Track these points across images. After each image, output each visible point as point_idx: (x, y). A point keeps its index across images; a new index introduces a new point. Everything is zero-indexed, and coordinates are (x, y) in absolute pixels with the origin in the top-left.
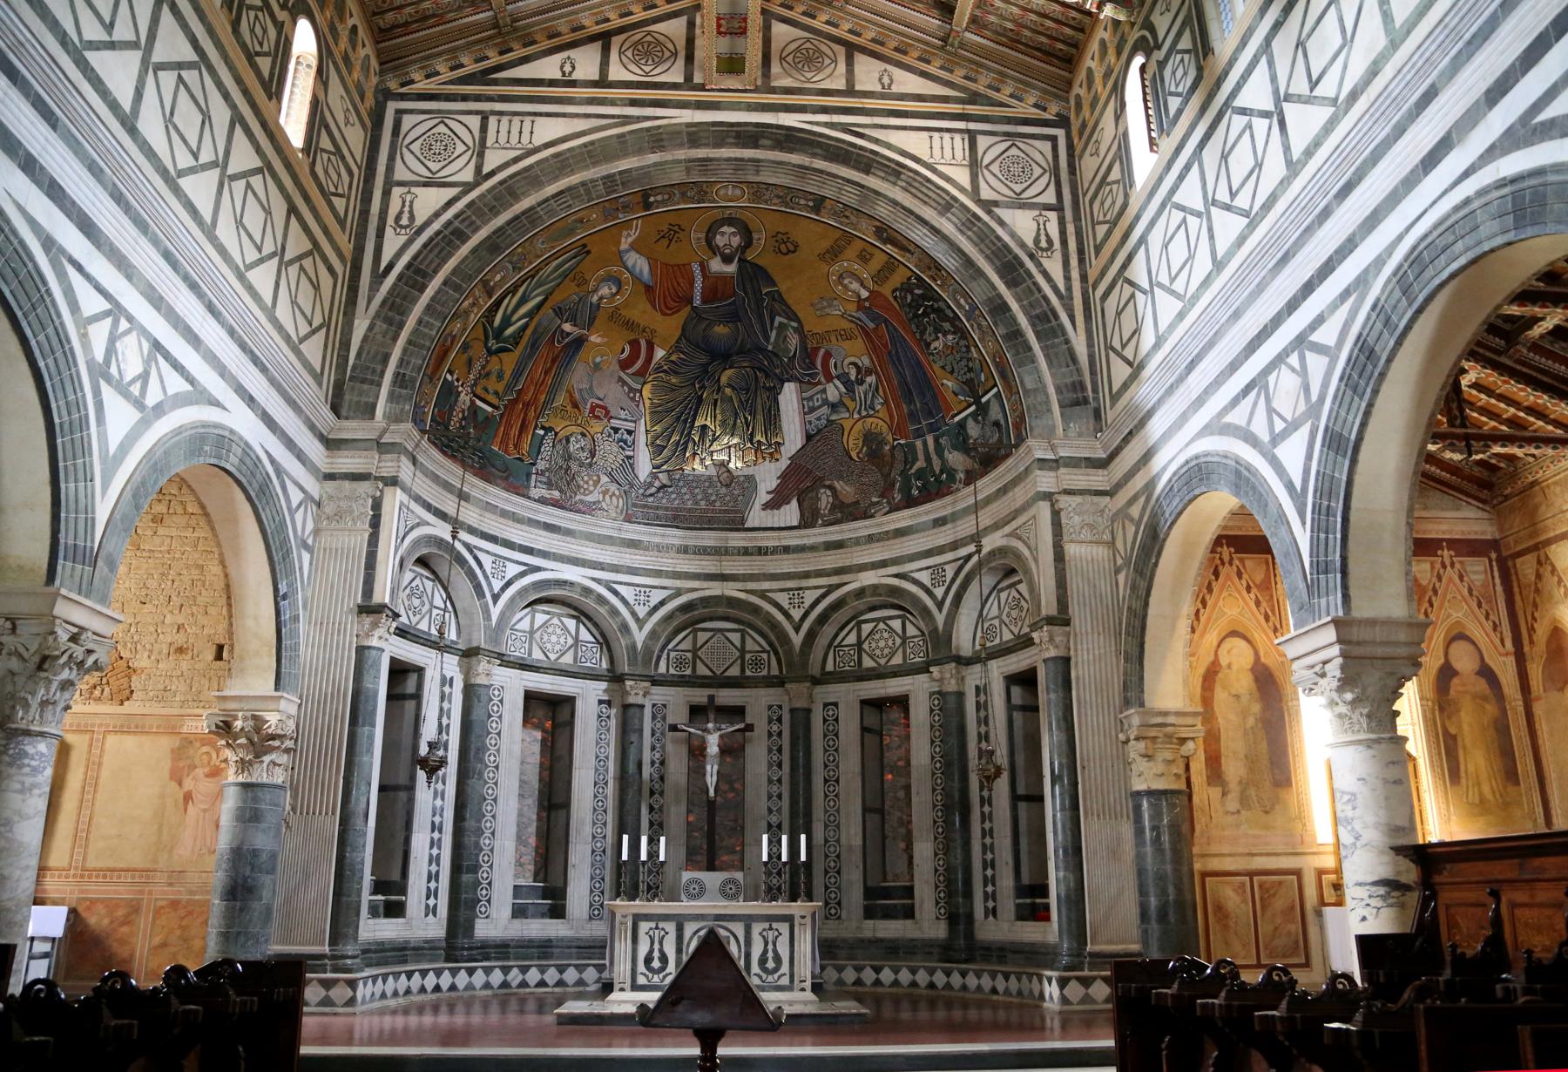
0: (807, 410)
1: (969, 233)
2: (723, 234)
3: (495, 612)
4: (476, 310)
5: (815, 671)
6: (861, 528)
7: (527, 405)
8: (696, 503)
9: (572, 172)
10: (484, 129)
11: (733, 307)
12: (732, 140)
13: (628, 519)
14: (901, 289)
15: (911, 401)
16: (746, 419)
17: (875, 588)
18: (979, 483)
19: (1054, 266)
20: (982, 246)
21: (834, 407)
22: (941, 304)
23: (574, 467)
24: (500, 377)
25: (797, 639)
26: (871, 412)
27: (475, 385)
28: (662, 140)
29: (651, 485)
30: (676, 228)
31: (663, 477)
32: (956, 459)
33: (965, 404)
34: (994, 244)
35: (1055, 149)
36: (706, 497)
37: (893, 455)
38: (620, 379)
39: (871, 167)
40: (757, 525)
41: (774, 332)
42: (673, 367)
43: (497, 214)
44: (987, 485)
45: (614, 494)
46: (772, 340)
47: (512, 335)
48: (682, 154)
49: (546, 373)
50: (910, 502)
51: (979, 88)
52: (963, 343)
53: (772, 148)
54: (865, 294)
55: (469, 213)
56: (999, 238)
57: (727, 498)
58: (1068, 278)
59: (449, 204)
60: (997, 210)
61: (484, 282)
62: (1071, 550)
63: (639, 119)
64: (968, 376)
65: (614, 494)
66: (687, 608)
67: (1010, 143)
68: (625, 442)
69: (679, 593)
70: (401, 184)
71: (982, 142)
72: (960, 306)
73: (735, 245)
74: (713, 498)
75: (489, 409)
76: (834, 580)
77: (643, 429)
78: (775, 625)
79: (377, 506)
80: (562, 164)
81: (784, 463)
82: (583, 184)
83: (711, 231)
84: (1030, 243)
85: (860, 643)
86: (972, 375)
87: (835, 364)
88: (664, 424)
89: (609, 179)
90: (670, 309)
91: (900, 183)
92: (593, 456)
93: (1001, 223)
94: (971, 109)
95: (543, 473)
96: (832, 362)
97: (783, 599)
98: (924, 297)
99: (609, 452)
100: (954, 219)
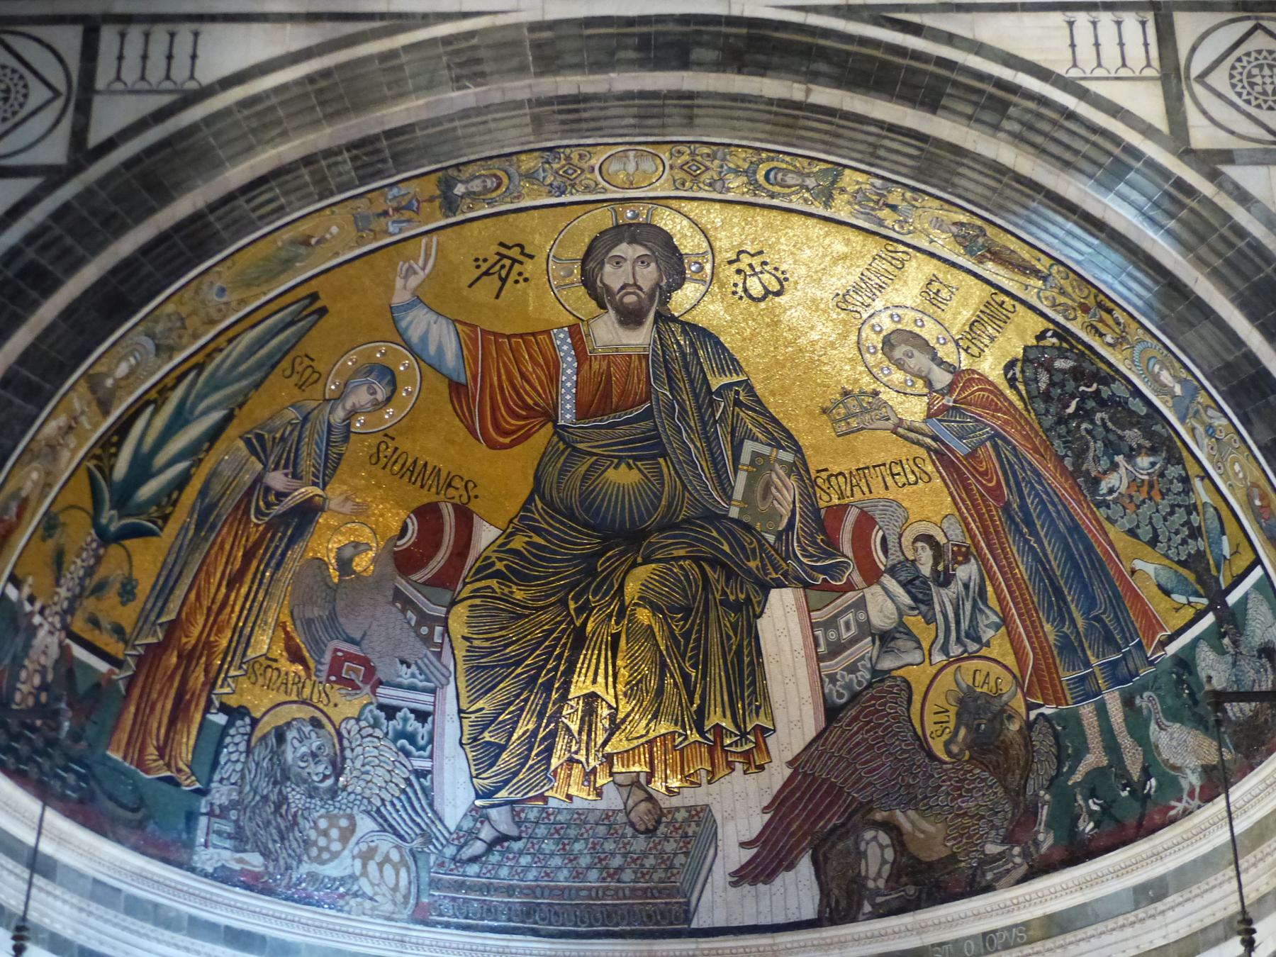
1: (1172, 224)
2: (619, 261)
4: (72, 441)
7: (188, 658)
8: (578, 875)
9: (284, 136)
11: (650, 424)
12: (632, 54)
14: (1026, 360)
15: (1061, 615)
16: (686, 677)
18: (1238, 792)
20: (1203, 251)
21: (885, 639)
22: (1119, 389)
23: (296, 798)
24: (127, 592)
26: (973, 647)
27: (70, 611)
28: (478, 61)
29: (472, 835)
30: (515, 253)
33: (1189, 613)
34: (1231, 245)
36: (600, 861)
37: (1028, 742)
38: (398, 595)
39: (941, 95)
40: (720, 922)
41: (742, 476)
42: (517, 564)
43: (120, 230)
45: (387, 859)
46: (738, 493)
47: (155, 500)
48: (523, 87)
49: (230, 587)
52: (1173, 471)
53: (719, 66)
54: (942, 378)
55: (58, 231)
56: (1240, 232)
57: (650, 862)
60: (1231, 171)
61: (93, 381)
64: (1192, 547)
65: (387, 859)
67: (1249, 25)
68: (411, 738)
72: (1162, 389)
73: (646, 285)
74: (617, 862)
75: (103, 666)
77: (451, 707)
81: (777, 774)
82: (308, 160)
86: (1202, 544)
87: (884, 539)
88: (499, 695)
90: (506, 433)
91: (1006, 124)
92: (338, 771)
93: (1244, 198)
95: (223, 812)
96: (877, 537)
98: (1077, 374)
100: (1135, 196)
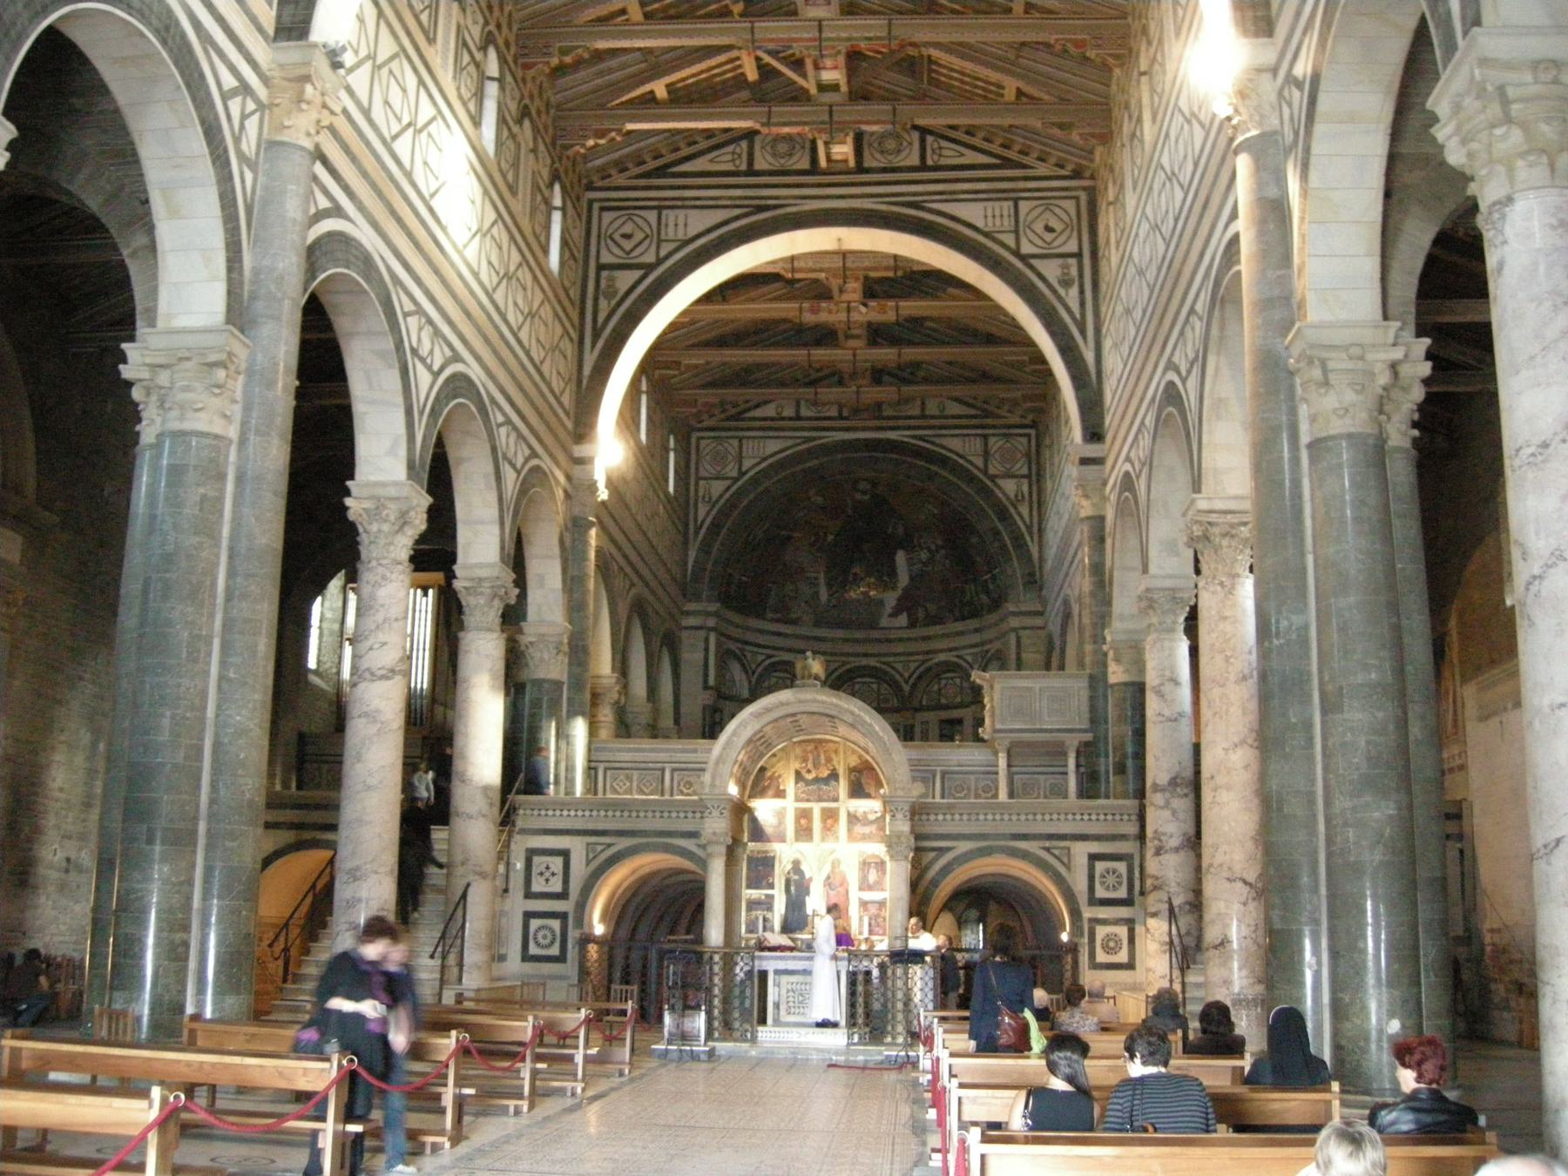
0: (910, 562)
3: (754, 680)
5: (915, 703)
6: (937, 629)
10: (741, 447)
13: (817, 624)
17: (946, 663)
19: (1024, 511)
25: (907, 688)
31: (834, 602)
32: (984, 597)
35: (1029, 442)
44: (993, 617)
50: (964, 619)
51: (991, 408)
58: (1031, 515)
59: (728, 489)
62: (1024, 656)
63: (820, 438)
66: (849, 671)
69: (844, 663)
70: (705, 479)
71: (992, 440)
76: (926, 657)
78: (896, 682)
79: (707, 640)
80: (781, 465)
81: (899, 592)
83: (856, 482)
84: (1012, 496)
85: (940, 690)
89: (804, 471)
93: (999, 488)
94: (989, 421)
97: (899, 667)
99: (806, 590)
